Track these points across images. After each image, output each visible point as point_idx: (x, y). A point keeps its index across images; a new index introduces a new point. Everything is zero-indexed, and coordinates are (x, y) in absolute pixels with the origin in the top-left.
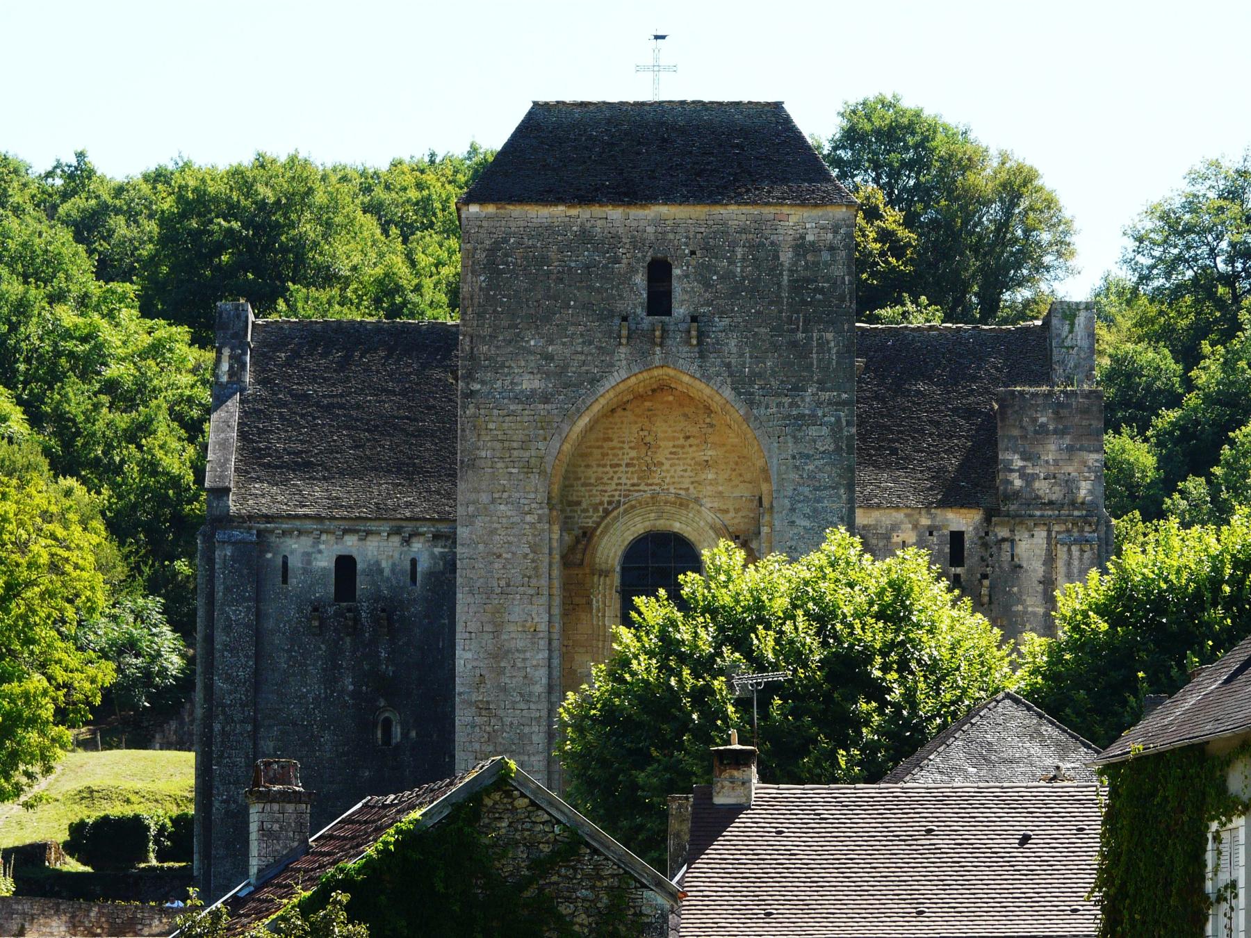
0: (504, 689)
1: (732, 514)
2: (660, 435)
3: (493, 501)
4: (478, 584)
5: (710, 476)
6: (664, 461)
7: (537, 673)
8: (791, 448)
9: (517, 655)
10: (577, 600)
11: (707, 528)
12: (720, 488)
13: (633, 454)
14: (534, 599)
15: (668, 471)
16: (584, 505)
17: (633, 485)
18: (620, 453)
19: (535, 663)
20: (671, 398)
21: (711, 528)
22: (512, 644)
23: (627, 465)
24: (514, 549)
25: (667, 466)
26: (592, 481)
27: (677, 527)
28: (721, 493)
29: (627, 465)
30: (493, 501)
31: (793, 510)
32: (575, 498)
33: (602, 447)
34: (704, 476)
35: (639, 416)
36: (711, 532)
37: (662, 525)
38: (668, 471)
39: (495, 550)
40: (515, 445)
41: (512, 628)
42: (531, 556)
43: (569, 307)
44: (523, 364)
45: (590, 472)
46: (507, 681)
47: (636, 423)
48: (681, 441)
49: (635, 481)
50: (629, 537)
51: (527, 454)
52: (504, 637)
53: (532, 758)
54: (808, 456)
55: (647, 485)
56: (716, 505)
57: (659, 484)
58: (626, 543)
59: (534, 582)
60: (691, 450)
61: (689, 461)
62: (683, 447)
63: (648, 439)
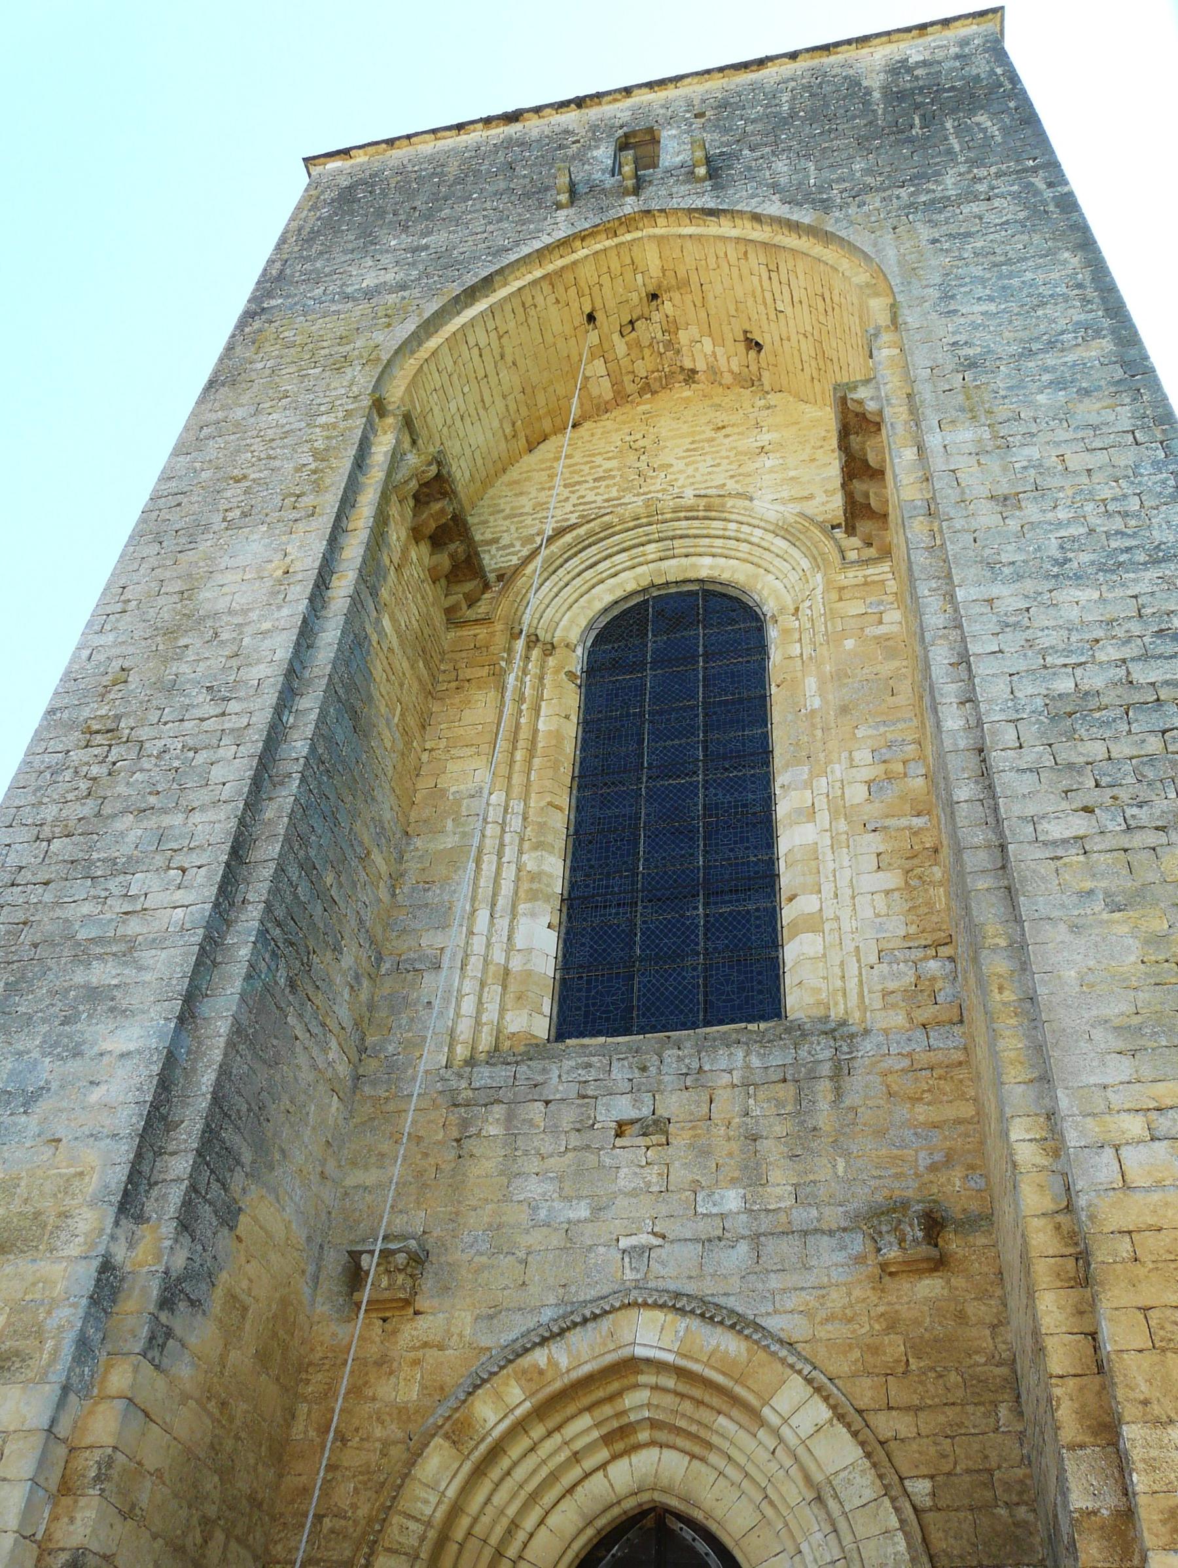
0: (172, 688)
1: (821, 498)
2: (664, 433)
3: (257, 412)
4: (178, 527)
5: (768, 464)
6: (674, 462)
7: (268, 643)
8: (925, 233)
9: (225, 618)
10: (468, 673)
11: (770, 537)
12: (792, 473)
13: (608, 465)
14: (300, 526)
15: (681, 472)
16: (505, 541)
17: (607, 501)
18: (586, 468)
19: (266, 626)
20: (687, 393)
21: (782, 530)
22: (222, 605)
23: (595, 480)
24: (277, 463)
25: (679, 465)
26: (527, 509)
27: (705, 567)
28: (792, 479)
29: (595, 480)
30: (257, 412)
31: (947, 297)
32: (488, 536)
33: (552, 467)
34: (757, 465)
35: (624, 423)
36: (781, 544)
37: (674, 570)
38: (681, 472)
39: (236, 472)
40: (325, 344)
41: (229, 577)
42: (313, 466)
43: (469, 198)
44: (370, 263)
45: (523, 500)
46: (184, 668)
47: (617, 430)
48: (710, 434)
49: (614, 494)
50: (604, 596)
51: (348, 348)
52: (205, 594)
53: (197, 817)
54: (968, 235)
55: (638, 495)
56: (785, 494)
57: (664, 490)
58: (599, 606)
59: (308, 501)
60: (727, 441)
61: (724, 453)
62: (713, 439)
63: (641, 443)
